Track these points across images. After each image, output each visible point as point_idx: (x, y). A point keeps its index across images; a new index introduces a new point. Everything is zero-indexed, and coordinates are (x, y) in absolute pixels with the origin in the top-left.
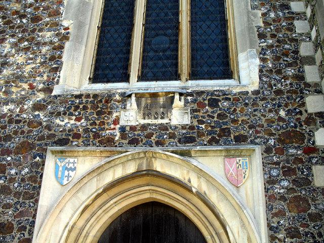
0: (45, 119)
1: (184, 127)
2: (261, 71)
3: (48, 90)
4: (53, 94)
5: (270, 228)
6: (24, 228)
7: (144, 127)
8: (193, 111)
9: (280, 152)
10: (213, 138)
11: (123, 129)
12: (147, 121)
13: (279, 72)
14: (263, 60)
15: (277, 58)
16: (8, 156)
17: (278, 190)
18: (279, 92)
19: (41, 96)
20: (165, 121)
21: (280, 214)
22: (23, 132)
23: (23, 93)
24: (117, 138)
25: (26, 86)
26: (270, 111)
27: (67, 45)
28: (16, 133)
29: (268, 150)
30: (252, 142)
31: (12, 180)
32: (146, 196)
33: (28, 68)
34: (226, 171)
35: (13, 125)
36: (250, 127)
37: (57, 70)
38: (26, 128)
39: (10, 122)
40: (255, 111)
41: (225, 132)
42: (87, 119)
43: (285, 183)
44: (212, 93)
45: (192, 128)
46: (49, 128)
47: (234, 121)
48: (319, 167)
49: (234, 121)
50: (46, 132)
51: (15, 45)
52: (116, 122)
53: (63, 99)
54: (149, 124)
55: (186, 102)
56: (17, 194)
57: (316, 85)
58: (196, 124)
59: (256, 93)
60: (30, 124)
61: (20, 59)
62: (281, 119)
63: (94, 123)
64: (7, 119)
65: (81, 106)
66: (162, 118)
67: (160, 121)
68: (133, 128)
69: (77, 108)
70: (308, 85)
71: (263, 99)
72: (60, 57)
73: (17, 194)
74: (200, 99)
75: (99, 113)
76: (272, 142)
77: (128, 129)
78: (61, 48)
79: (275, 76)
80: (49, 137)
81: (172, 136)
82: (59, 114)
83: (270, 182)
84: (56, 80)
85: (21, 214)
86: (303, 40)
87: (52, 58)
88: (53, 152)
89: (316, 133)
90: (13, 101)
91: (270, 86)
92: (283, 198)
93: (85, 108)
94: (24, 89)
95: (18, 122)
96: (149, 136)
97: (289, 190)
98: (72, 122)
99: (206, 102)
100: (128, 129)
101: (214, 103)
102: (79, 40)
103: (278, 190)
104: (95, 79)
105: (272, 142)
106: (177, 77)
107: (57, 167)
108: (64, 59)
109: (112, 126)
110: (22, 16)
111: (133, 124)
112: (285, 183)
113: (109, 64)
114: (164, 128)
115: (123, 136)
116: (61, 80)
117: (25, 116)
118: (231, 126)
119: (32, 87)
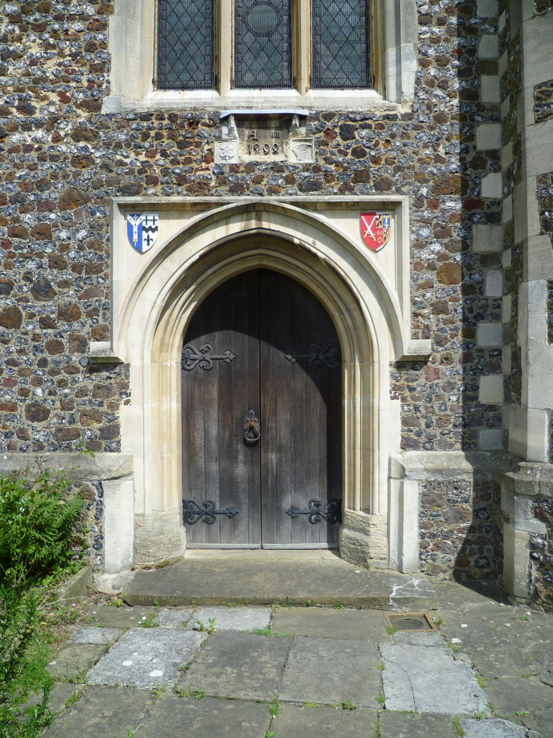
0: (98, 154)
1: (306, 168)
2: (418, 81)
3: (93, 105)
4: (104, 111)
5: (414, 303)
6: (96, 311)
7: (250, 167)
8: (320, 143)
9: (434, 205)
10: (345, 184)
12: (254, 158)
13: (443, 85)
14: (424, 64)
16: (51, 211)
17: (425, 254)
18: (440, 119)
19: (83, 115)
20: (278, 158)
21: (428, 285)
22: (65, 176)
23: (52, 109)
24: (213, 184)
25: (54, 97)
26: (426, 146)
27: (112, 20)
28: (54, 176)
29: (418, 203)
30: (398, 191)
31: (65, 248)
32: (253, 263)
33: (50, 68)
34: (363, 228)
35: (47, 165)
36: (398, 169)
37: (102, 68)
38: (70, 169)
39: (42, 159)
40: (405, 145)
41: (361, 177)
42: (164, 154)
43: (437, 247)
44: (347, 117)
45: (317, 169)
46: (106, 167)
47: (376, 160)
48: (481, 227)
49: (376, 160)
50: (104, 176)
52: (209, 158)
53: (123, 120)
54: (257, 164)
55: (310, 132)
56: (76, 268)
57: (495, 108)
58: (322, 162)
59: (407, 117)
62: (438, 159)
63: (175, 162)
64: (34, 154)
65: (152, 133)
66: (275, 153)
67: (271, 158)
68: (234, 168)
69: (146, 137)
70: (481, 108)
71: (416, 128)
72: (104, 45)
73: (76, 268)
74: (329, 125)
75: (182, 145)
76: (424, 191)
77: (227, 170)
78: (104, 26)
79: (439, 92)
80: (109, 183)
81: (290, 180)
82: (118, 146)
83: (419, 244)
84: (104, 86)
85: (87, 295)
86: (485, 31)
87: (91, 47)
88: (125, 208)
89: (484, 181)
90: (39, 125)
91: (429, 107)
92: (431, 267)
93: (158, 136)
94: (52, 103)
95: (54, 158)
96: (258, 181)
97: (442, 257)
98: (142, 158)
99: (337, 130)
100: (227, 170)
101: (347, 133)
103: (425, 254)
104: (162, 84)
105: (424, 191)
106: (293, 83)
107: (130, 227)
108: (112, 48)
109: (204, 165)
111: (234, 161)
112: (437, 247)
113: (183, 56)
114: (277, 168)
115: (222, 182)
116: (113, 87)
117: (64, 148)
119: (65, 99)
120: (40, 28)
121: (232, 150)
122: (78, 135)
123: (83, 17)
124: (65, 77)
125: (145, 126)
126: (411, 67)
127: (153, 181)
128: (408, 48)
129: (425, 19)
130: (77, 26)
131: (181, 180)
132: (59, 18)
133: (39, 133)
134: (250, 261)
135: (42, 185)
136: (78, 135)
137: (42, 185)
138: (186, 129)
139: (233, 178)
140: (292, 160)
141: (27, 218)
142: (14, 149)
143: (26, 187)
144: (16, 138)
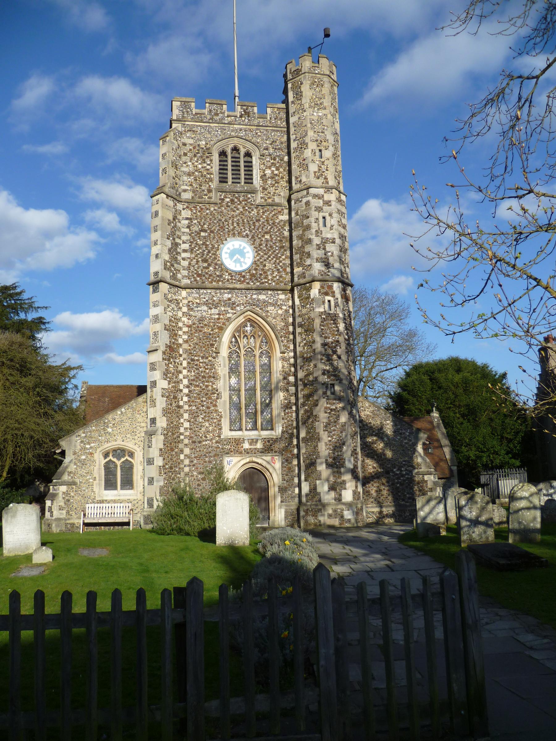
7: (250, 449)
11: (244, 449)
14: (283, 427)
15: (286, 427)
19: (217, 438)
25: (211, 435)
27: (223, 420)
33: (211, 428)
37: (221, 429)
39: (209, 447)
46: (222, 449)
51: (203, 418)
52: (242, 447)
60: (216, 448)
61: (207, 424)
67: (254, 447)
68: (247, 449)
75: (237, 444)
81: (258, 451)
83: (283, 463)
87: (218, 425)
96: (252, 451)
97: (287, 465)
101: (269, 441)
102: (225, 418)
110: (203, 406)
113: (236, 424)
114: (256, 449)
115: (245, 452)
118: (273, 448)
119: (213, 435)
120: (208, 421)
121: (246, 446)
122: (217, 442)
123: (217, 419)
124: (214, 431)
125: (229, 441)
126: (281, 428)
127: (232, 452)
128: (280, 425)
129: (283, 419)
130: (215, 421)
131: (237, 451)
132: (212, 418)
133: (209, 442)
134: (250, 465)
135: (210, 452)
136: (217, 442)
137: (210, 452)
138: (238, 442)
139: (247, 452)
140: (258, 447)
141: (207, 459)
142: (204, 445)
143: (207, 453)
144: (204, 443)
